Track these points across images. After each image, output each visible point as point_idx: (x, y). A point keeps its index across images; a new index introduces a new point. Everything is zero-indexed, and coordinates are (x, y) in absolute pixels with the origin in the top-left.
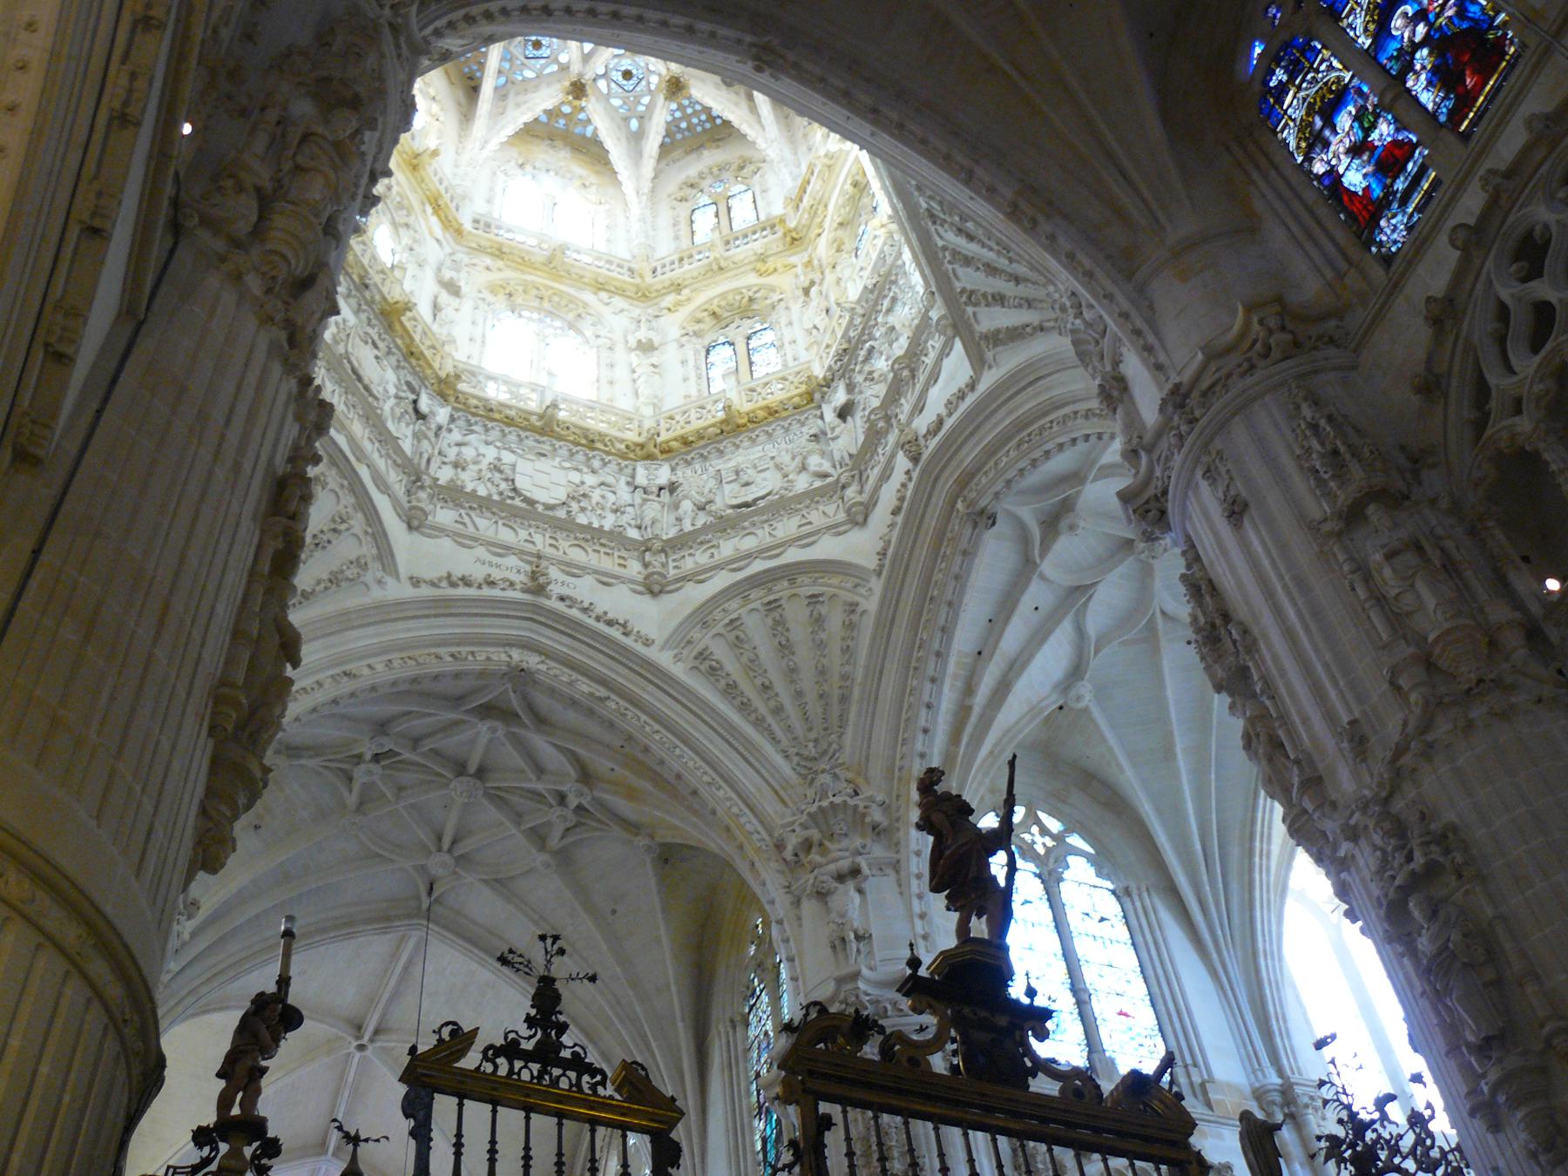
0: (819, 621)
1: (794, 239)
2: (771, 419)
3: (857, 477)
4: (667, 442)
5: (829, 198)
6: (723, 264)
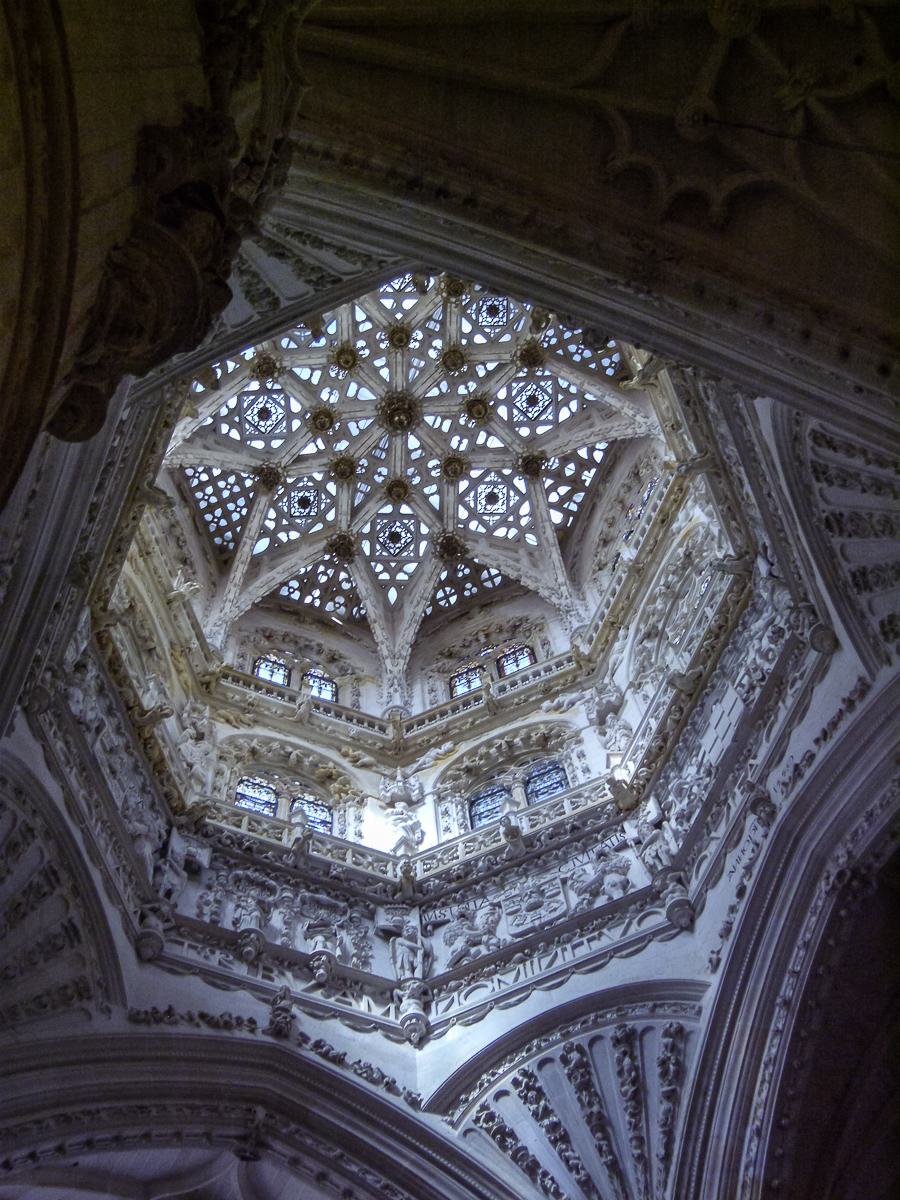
0: (50, 948)
1: (208, 685)
2: (151, 766)
3: (168, 925)
4: (110, 639)
5: (265, 725)
6: (175, 604)
